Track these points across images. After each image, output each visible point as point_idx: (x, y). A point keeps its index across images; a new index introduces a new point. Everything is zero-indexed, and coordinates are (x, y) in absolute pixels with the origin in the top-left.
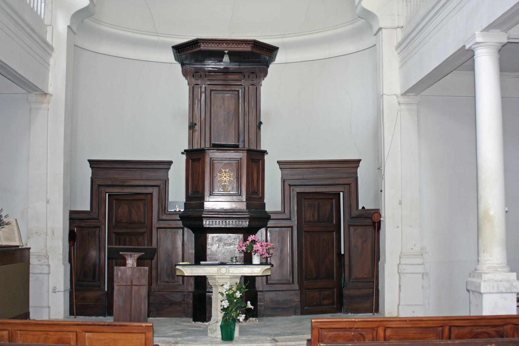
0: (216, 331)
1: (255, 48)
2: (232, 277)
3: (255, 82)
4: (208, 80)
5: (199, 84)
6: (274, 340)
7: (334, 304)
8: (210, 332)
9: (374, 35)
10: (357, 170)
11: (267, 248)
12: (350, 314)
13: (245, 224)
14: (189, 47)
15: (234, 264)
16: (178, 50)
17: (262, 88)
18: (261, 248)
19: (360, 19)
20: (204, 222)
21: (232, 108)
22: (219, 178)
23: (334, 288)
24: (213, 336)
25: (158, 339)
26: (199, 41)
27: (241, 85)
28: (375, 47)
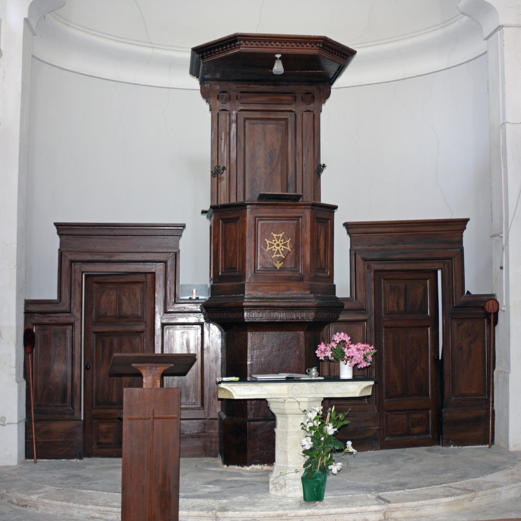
0: (286, 487)
1: (324, 50)
2: (312, 400)
3: (311, 107)
4: (242, 103)
5: (228, 109)
6: (379, 498)
7: (427, 432)
8: (275, 489)
9: (485, 39)
10: (462, 237)
11: (365, 353)
12: (452, 447)
13: (309, 316)
14: (224, 48)
15: (313, 378)
16: (202, 53)
17: (322, 115)
18: (358, 353)
19: (462, 15)
20: (245, 314)
21: (278, 146)
22: (269, 247)
23: (429, 409)
24: (279, 494)
25: (190, 503)
26: (238, 38)
27: (291, 111)
28: (485, 55)
